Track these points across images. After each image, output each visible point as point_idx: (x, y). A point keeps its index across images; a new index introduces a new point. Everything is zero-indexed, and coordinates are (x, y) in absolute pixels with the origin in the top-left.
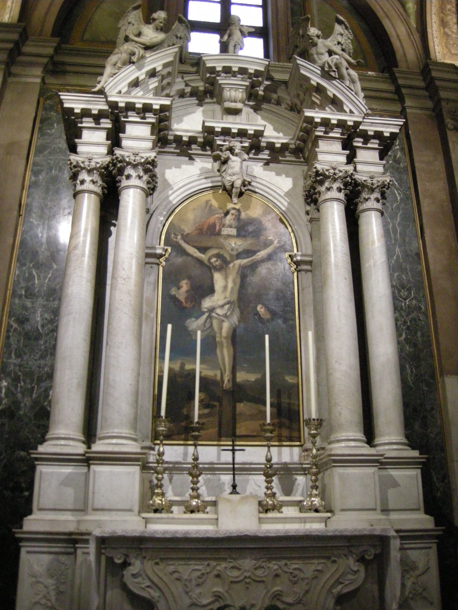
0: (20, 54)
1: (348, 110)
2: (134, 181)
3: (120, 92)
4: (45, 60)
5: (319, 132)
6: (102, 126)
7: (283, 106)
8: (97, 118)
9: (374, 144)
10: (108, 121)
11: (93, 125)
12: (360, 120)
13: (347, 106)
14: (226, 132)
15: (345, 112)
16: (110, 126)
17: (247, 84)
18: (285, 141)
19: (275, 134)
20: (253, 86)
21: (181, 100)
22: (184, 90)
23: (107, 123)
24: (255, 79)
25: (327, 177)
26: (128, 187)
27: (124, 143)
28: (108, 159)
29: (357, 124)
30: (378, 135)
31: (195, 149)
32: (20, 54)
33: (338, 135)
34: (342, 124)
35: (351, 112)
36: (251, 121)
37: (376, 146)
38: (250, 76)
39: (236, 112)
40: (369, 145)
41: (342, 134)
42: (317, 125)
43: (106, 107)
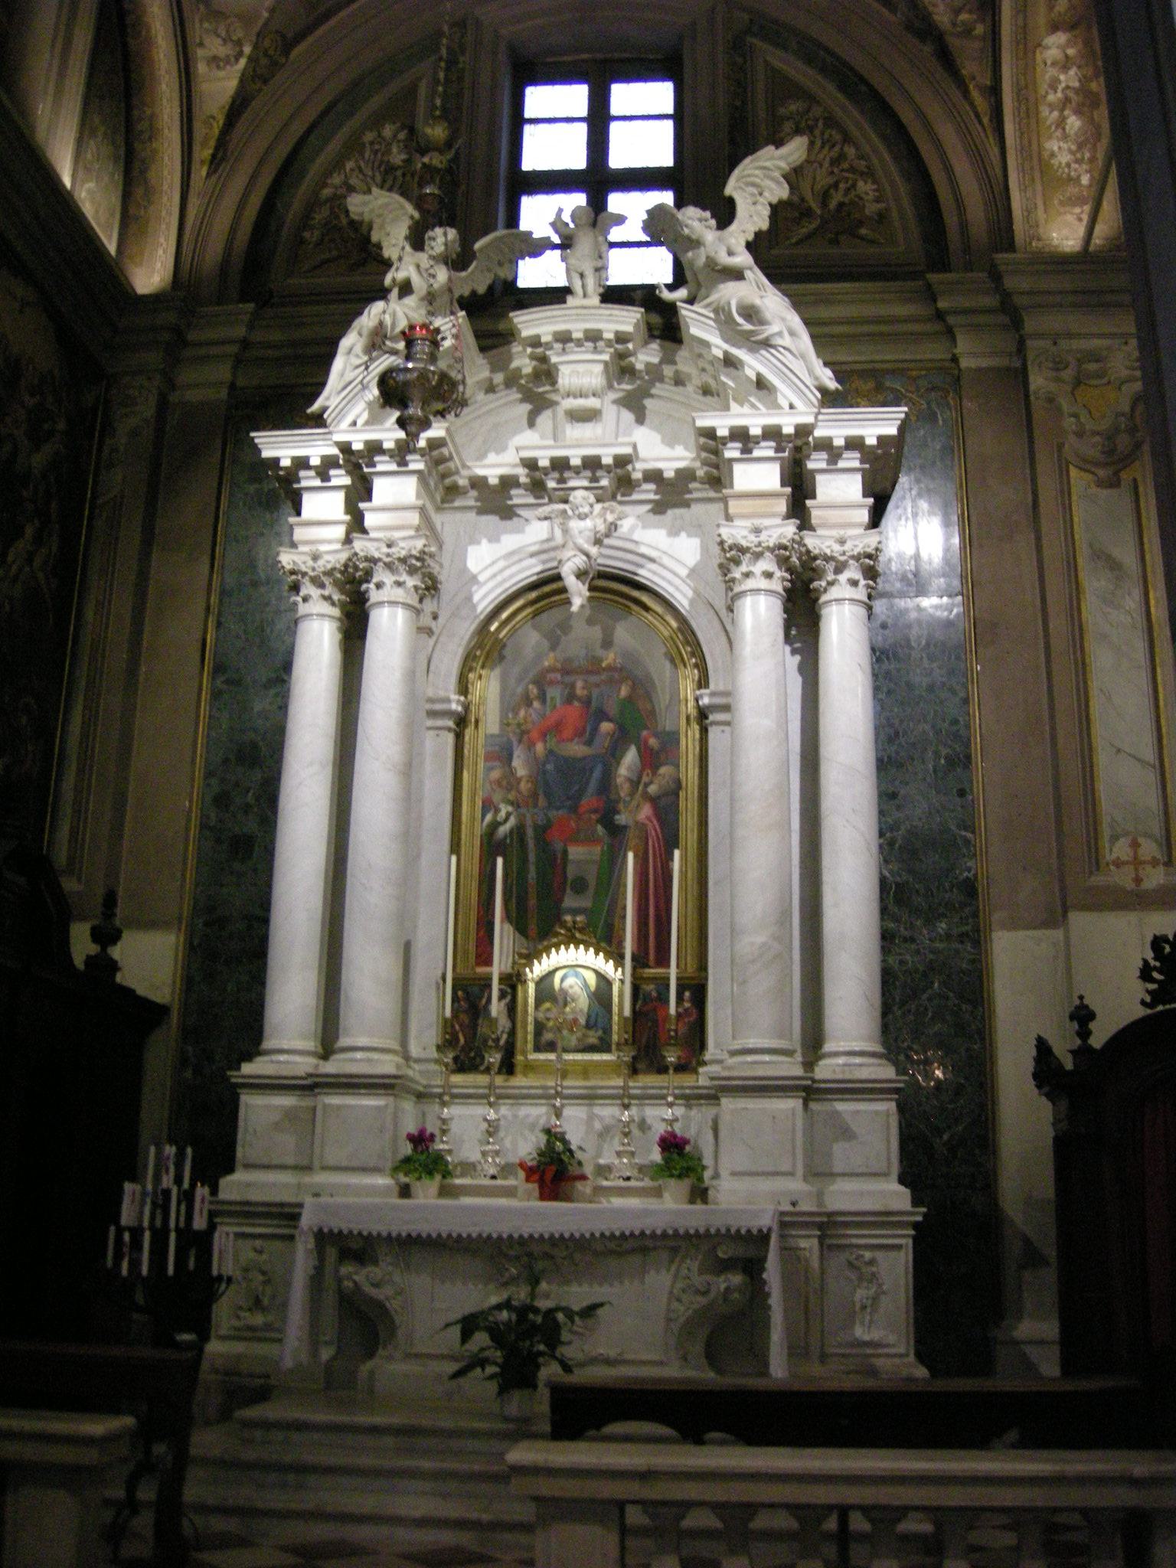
0: (186, 344)
1: (786, 405)
2: (389, 592)
3: (354, 424)
4: (233, 349)
5: (732, 452)
6: (334, 482)
7: (690, 388)
8: (323, 472)
9: (851, 460)
10: (342, 472)
11: (317, 483)
12: (810, 419)
13: (785, 397)
14: (560, 465)
15: (779, 407)
16: (347, 481)
17: (606, 357)
18: (682, 464)
19: (666, 452)
20: (621, 356)
21: (491, 396)
22: (491, 380)
23: (341, 478)
24: (619, 347)
25: (743, 550)
26: (381, 604)
27: (370, 520)
28: (344, 556)
29: (803, 431)
30: (854, 444)
31: (519, 497)
32: (186, 344)
33: (771, 453)
34: (772, 433)
35: (791, 407)
36: (610, 435)
37: (856, 464)
38: (609, 343)
39: (587, 416)
40: (841, 464)
41: (777, 450)
42: (724, 441)
43: (335, 451)
